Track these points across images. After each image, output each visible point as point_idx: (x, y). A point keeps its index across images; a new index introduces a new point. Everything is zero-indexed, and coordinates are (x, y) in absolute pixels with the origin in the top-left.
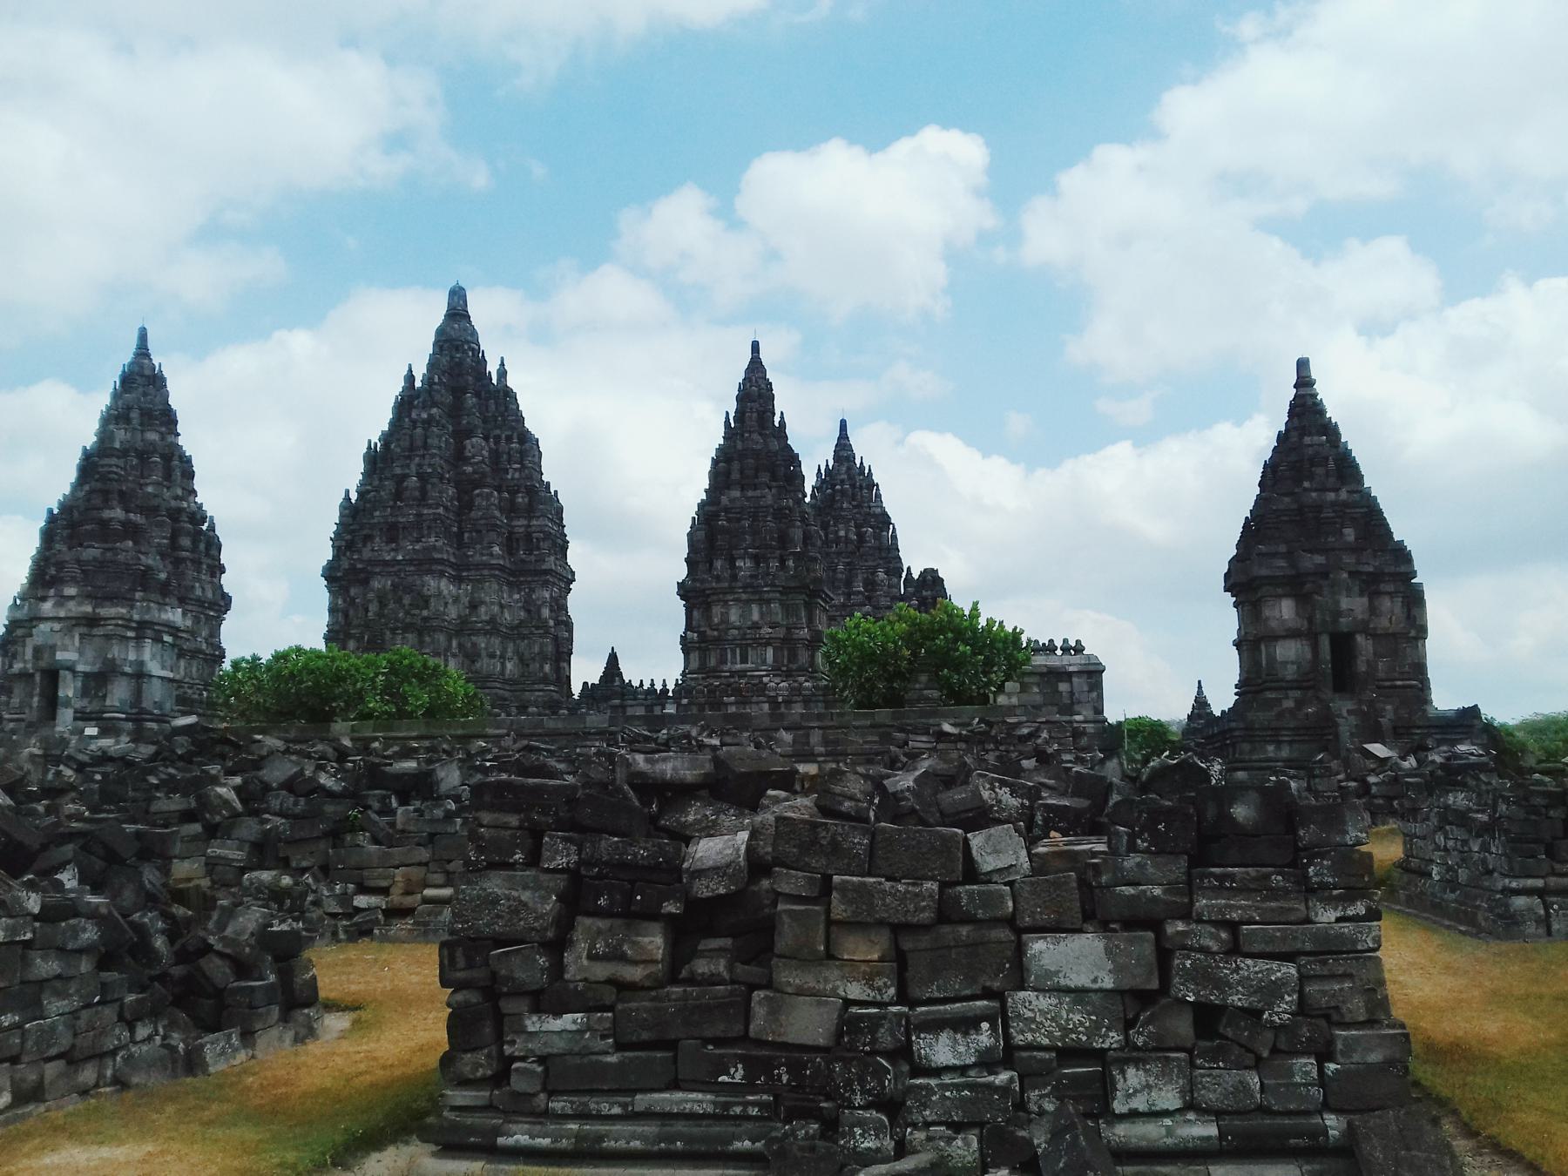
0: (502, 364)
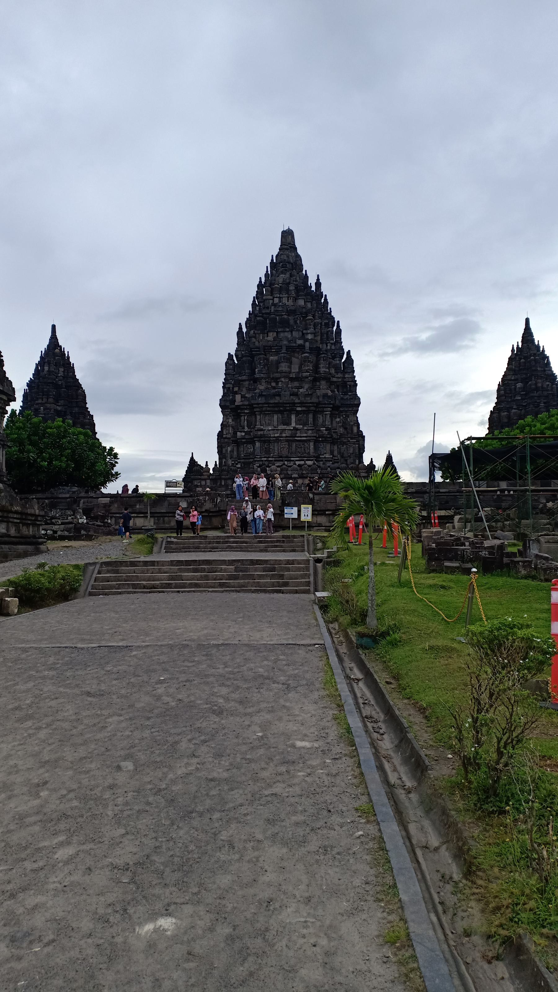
0: (318, 279)
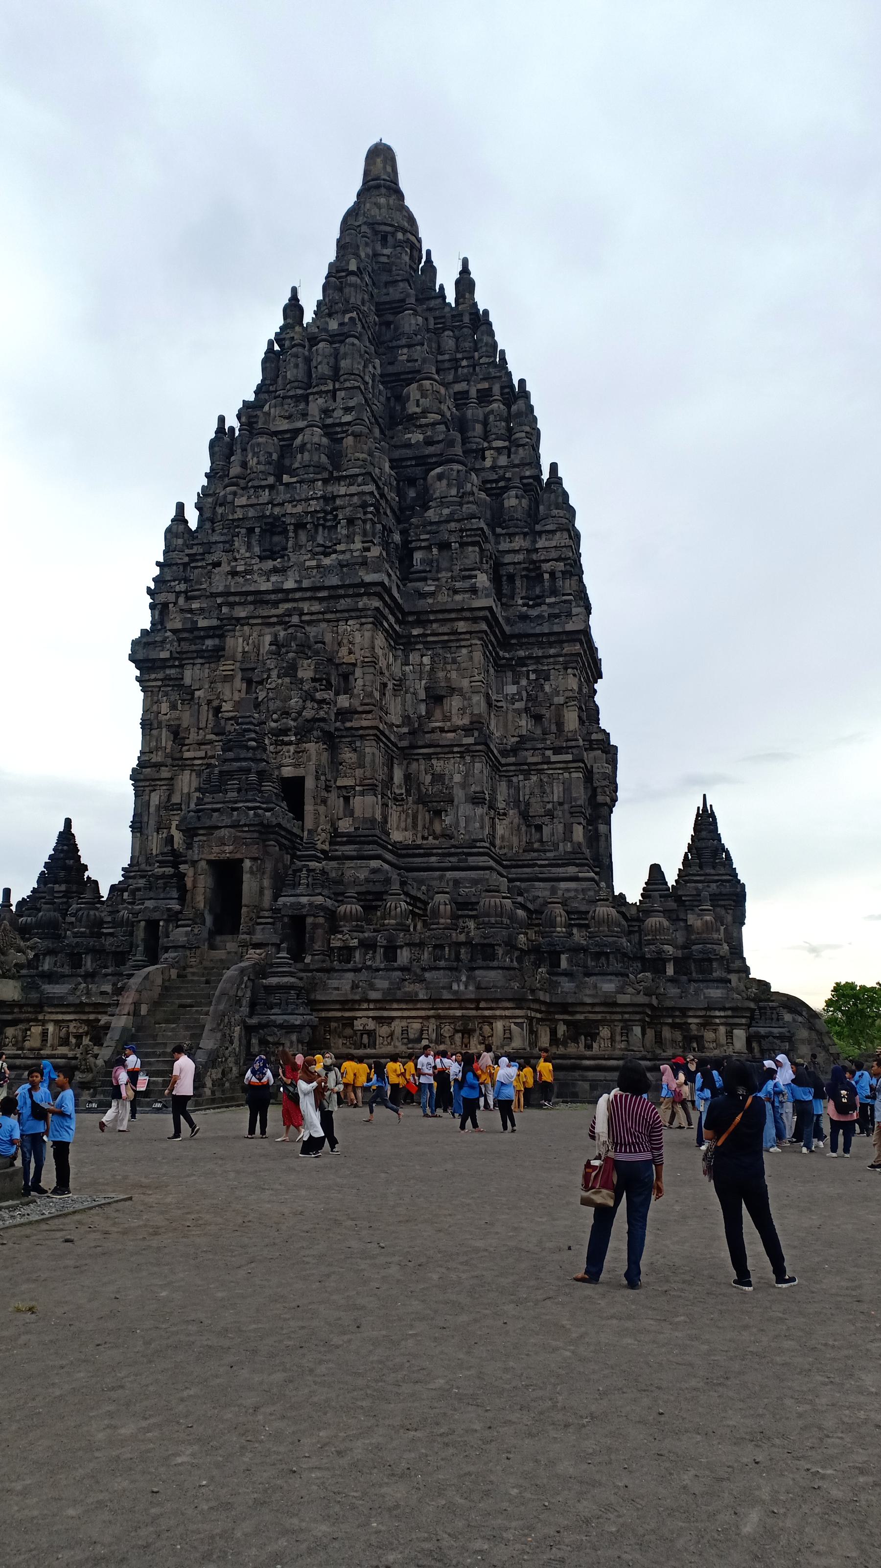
0: (465, 271)
